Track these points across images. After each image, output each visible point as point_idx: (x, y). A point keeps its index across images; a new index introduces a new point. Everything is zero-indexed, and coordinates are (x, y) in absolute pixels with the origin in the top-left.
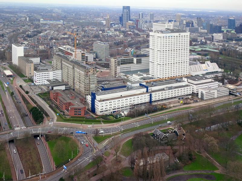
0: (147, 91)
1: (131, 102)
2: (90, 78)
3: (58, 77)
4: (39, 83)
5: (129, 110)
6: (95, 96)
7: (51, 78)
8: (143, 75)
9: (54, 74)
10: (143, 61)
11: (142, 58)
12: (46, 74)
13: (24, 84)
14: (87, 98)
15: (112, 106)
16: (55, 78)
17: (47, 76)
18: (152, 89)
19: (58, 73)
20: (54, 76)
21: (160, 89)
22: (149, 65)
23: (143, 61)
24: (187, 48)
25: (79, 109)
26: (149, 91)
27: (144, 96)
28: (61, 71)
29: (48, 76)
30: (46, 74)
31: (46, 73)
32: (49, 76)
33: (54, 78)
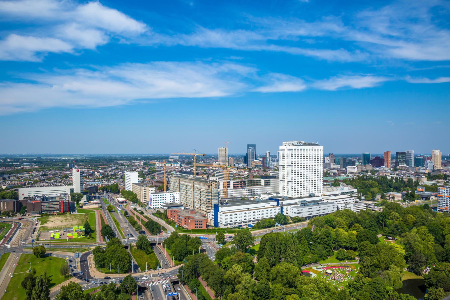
0: (278, 205)
4: (154, 207)
5: (256, 222)
7: (168, 201)
8: (272, 194)
10: (272, 182)
11: (271, 179)
13: (138, 208)
14: (209, 216)
15: (238, 220)
17: (163, 199)
18: (283, 202)
23: (272, 182)
24: (321, 164)
25: (200, 222)
26: (280, 205)
27: (274, 210)
28: (179, 193)
29: (165, 198)
30: (163, 196)
31: (163, 194)
32: (165, 198)
33: (171, 200)
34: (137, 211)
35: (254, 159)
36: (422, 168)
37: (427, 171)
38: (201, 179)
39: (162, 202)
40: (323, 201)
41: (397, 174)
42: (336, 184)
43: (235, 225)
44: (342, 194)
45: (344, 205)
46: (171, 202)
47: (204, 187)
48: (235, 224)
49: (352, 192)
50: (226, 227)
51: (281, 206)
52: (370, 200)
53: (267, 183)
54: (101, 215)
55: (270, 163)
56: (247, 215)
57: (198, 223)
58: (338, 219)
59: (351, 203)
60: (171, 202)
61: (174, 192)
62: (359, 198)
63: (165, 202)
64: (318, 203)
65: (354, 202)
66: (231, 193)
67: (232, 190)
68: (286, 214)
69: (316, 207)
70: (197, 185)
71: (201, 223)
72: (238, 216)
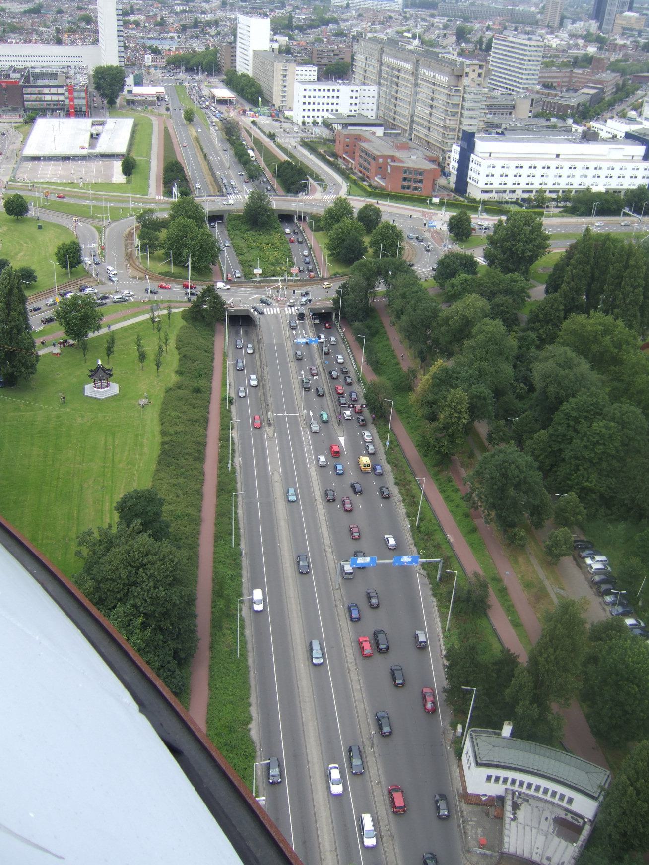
1: (584, 180)
2: (466, 96)
3: (365, 106)
6: (474, 143)
7: (345, 109)
9: (354, 94)
12: (331, 94)
15: (523, 181)
16: (356, 108)
17: (330, 100)
19: (366, 93)
20: (354, 101)
28: (376, 88)
29: (335, 101)
30: (331, 94)
33: (354, 107)
38: (440, 55)
39: (328, 110)
43: (510, 195)
46: (353, 113)
48: (514, 192)
50: (486, 197)
54: (166, 130)
56: (552, 172)
60: (351, 111)
61: (364, 84)
63: (337, 110)
70: (426, 73)
72: (525, 171)
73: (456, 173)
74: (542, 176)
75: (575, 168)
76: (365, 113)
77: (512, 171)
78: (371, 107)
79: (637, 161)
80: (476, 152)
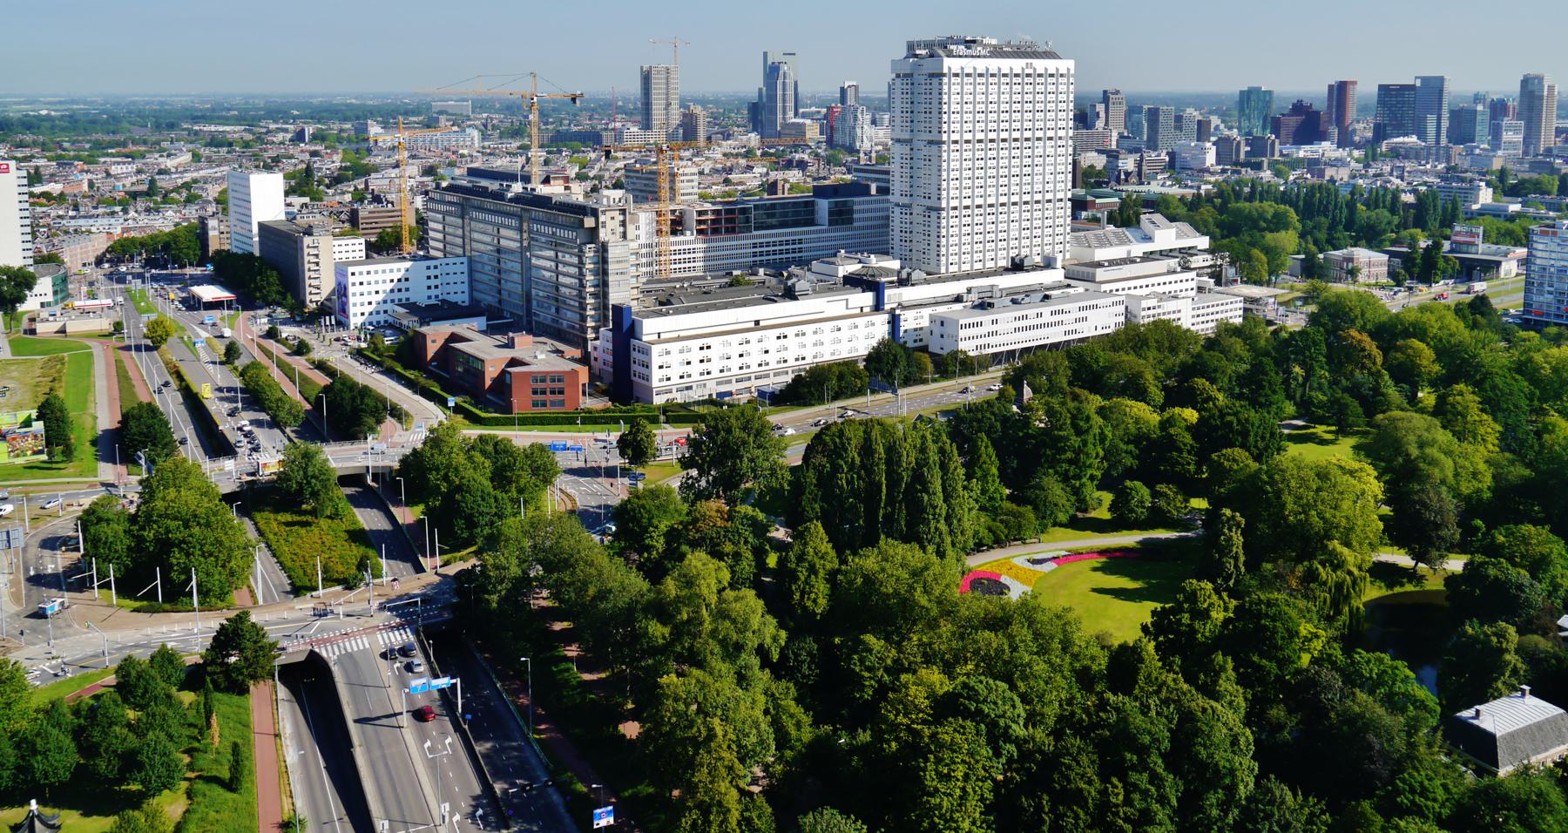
0: (878, 307)
3: (452, 288)
9: (432, 272)
16: (438, 292)
19: (451, 269)
20: (433, 282)
21: (939, 300)
22: (887, 226)
23: (860, 211)
25: (553, 380)
26: (887, 307)
33: (433, 292)
34: (284, 342)
35: (791, 114)
36: (1477, 151)
37: (1497, 164)
40: (1069, 286)
41: (1375, 175)
42: (1126, 217)
44: (1148, 257)
45: (1153, 302)
46: (433, 302)
47: (570, 234)
49: (1190, 248)
51: (893, 309)
52: (1258, 283)
53: (840, 213)
55: (859, 131)
57: (549, 385)
58: (1128, 358)
59: (1183, 294)
60: (429, 297)
62: (1218, 277)
64: (1047, 297)
65: (1193, 293)
66: (687, 256)
67: (691, 246)
68: (915, 341)
69: (1039, 310)
71: (557, 385)
73: (611, 370)
74: (741, 356)
75: (785, 337)
76: (452, 298)
77: (696, 355)
78: (460, 288)
79: (867, 315)
80: (638, 335)
